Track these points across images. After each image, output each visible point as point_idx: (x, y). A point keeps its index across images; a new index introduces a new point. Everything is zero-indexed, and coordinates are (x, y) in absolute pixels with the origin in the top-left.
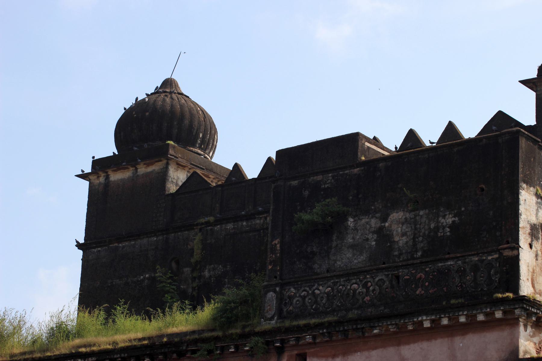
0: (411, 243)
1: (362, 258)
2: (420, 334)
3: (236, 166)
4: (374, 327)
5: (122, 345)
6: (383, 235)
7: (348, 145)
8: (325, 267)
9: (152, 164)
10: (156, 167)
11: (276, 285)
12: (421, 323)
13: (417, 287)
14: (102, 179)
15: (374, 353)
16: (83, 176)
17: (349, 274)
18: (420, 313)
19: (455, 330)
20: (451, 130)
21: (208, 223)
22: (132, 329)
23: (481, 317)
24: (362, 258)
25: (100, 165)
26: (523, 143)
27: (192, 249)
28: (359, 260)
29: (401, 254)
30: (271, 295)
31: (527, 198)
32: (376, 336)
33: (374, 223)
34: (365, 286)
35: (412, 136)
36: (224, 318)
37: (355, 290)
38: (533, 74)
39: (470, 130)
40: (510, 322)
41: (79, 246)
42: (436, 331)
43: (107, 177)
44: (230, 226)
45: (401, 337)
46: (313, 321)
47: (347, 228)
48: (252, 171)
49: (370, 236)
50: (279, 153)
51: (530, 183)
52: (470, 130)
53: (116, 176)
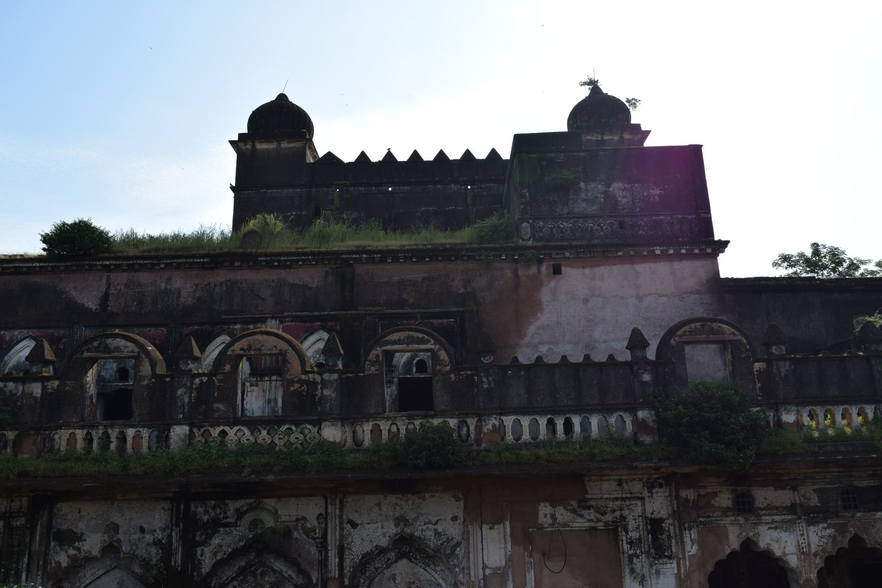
0: (630, 202)
1: (595, 208)
2: (652, 257)
4: (617, 251)
5: (406, 248)
8: (565, 211)
9: (294, 142)
11: (530, 218)
12: (654, 251)
13: (639, 230)
14: (249, 147)
15: (614, 267)
17: (586, 217)
18: (656, 245)
21: (345, 185)
24: (595, 208)
27: (333, 200)
28: (593, 209)
29: (623, 210)
30: (525, 224)
32: (620, 256)
34: (599, 225)
37: (592, 228)
42: (665, 257)
43: (254, 146)
44: (362, 189)
47: (580, 188)
49: (599, 195)
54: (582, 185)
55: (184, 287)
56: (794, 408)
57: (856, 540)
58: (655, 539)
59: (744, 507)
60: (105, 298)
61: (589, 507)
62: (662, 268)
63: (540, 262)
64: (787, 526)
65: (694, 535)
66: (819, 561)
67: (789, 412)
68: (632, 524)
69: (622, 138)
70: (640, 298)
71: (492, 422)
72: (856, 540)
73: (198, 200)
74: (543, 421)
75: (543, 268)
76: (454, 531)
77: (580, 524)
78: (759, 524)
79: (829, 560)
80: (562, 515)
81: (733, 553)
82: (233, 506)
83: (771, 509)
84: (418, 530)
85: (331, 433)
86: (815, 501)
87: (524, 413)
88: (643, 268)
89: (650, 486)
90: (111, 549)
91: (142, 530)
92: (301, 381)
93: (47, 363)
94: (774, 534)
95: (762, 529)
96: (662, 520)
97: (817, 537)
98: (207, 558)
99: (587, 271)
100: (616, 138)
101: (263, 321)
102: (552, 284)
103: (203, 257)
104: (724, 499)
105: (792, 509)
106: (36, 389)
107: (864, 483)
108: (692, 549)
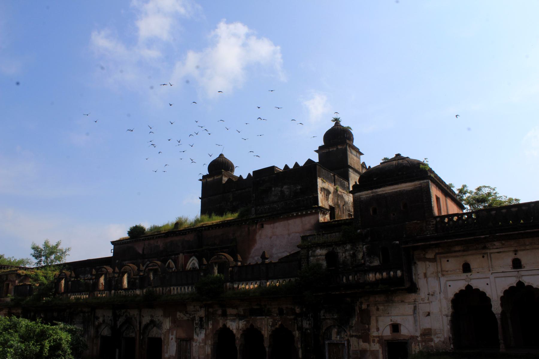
2: (293, 217)
3: (241, 176)
6: (282, 192)
7: (272, 169)
10: (219, 177)
15: (281, 223)
16: (200, 180)
19: (302, 216)
20: (296, 164)
22: (217, 219)
23: (309, 212)
25: (204, 177)
26: (318, 167)
31: (319, 181)
33: (279, 189)
35: (286, 167)
36: (241, 216)
38: (317, 149)
39: (301, 164)
40: (317, 213)
41: (200, 198)
42: (297, 216)
44: (239, 191)
45: (288, 218)
46: (265, 215)
48: (245, 177)
50: (254, 172)
51: (320, 177)
52: (301, 164)
53: (209, 180)
54: (273, 189)
55: (160, 243)
56: (238, 283)
57: (252, 326)
58: (201, 323)
59: (224, 315)
60: (143, 250)
61: (187, 313)
62: (298, 221)
63: (256, 223)
64: (233, 320)
65: (211, 322)
66: (241, 332)
67: (236, 284)
68: (197, 318)
69: (337, 148)
70: (289, 235)
71: (168, 288)
72: (252, 326)
73: (185, 206)
74: (179, 288)
75: (258, 226)
76: (161, 319)
77: (185, 318)
78: (227, 320)
79: (244, 331)
80: (182, 315)
81: (220, 328)
82: (123, 311)
83: (231, 315)
84: (156, 319)
85: (138, 292)
86: (242, 313)
87: (175, 286)
88: (291, 222)
89: (201, 307)
90: (104, 321)
91: (108, 317)
92: (133, 278)
93: (73, 277)
94: (231, 323)
95: (228, 321)
96: (202, 318)
97: (242, 324)
98: (119, 324)
99: (272, 225)
100: (335, 149)
101: (179, 254)
102: (260, 232)
103: (163, 233)
104: (220, 312)
105: (235, 315)
106: (91, 282)
107: (255, 307)
108: (210, 327)
